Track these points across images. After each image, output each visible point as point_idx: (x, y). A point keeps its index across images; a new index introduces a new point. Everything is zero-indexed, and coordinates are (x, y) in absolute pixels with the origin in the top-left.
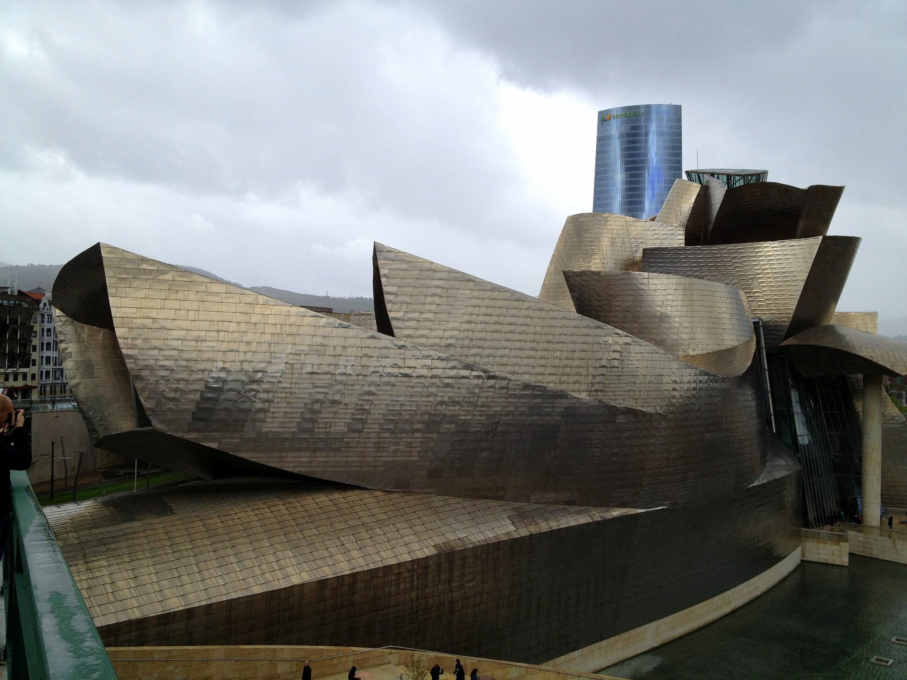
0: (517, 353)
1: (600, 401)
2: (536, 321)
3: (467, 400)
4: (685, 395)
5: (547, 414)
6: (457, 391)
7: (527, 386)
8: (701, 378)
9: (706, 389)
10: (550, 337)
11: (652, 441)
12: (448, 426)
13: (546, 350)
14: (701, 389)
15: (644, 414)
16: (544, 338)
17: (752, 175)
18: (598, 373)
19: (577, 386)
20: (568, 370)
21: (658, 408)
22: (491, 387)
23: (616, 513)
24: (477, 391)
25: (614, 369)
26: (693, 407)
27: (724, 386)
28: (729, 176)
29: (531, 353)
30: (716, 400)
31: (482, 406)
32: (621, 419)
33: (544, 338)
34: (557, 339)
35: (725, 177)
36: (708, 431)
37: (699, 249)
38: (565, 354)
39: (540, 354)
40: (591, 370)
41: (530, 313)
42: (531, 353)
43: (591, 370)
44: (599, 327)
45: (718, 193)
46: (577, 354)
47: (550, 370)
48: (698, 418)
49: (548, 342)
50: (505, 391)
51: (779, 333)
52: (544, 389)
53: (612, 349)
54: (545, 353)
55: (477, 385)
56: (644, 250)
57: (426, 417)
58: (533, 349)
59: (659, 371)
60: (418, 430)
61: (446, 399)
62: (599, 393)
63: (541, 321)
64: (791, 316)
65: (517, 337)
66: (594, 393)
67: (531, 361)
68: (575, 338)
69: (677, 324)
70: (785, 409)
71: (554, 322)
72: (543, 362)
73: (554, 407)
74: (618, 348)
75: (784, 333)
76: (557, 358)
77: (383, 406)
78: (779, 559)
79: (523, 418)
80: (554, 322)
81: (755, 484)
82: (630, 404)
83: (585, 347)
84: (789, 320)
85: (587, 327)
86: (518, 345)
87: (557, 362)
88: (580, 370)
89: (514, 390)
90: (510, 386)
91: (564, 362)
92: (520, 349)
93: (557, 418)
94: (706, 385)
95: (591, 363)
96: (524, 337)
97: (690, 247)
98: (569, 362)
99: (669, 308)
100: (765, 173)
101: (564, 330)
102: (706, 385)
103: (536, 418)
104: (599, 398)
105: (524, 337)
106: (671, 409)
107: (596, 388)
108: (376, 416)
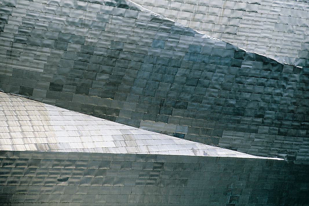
3: (96, 24)
5: (171, 48)
6: (87, 14)
7: (154, 19)
11: (278, 91)
12: (75, 46)
15: (274, 64)
18: (234, 15)
22: (121, 15)
24: (106, 17)
25: (253, 14)
31: (109, 32)
32: (247, 65)
40: (228, 12)
50: (132, 21)
55: (107, 12)
57: (56, 35)
60: (47, 46)
61: (77, 21)
62: (231, 36)
77: (20, 19)
79: (146, 49)
82: (260, 52)
89: (142, 21)
90: (138, 17)
93: (180, 54)
103: (158, 51)
107: (228, 30)
108: (11, 27)
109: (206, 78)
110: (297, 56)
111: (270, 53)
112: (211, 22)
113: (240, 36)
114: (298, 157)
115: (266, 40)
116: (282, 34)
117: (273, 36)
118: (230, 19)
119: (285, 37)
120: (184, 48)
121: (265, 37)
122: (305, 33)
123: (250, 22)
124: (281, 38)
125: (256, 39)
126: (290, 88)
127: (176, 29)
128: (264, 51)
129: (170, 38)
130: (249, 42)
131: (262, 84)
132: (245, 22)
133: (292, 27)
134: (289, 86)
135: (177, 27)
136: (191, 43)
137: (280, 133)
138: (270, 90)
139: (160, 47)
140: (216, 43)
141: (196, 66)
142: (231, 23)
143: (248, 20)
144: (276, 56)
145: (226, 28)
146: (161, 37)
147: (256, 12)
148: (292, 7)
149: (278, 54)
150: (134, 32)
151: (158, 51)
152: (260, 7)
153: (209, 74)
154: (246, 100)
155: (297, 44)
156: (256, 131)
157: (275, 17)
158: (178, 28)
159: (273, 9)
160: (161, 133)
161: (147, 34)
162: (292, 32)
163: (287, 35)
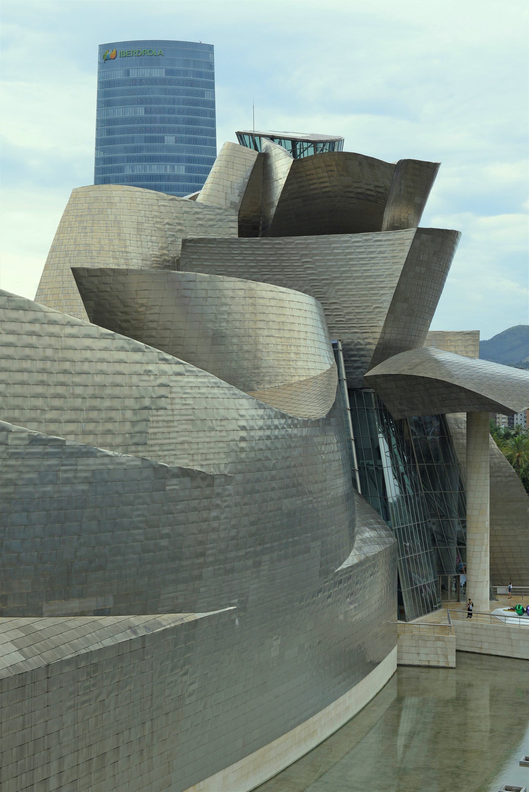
0: (18, 389)
1: (143, 459)
2: (47, 340)
4: (257, 447)
5: (67, 481)
7: (34, 441)
8: (276, 422)
9: (283, 437)
10: (67, 366)
11: (214, 514)
13: (63, 384)
14: (276, 437)
16: (57, 367)
17: (324, 142)
18: (138, 418)
19: (109, 439)
20: (94, 415)
21: (222, 467)
23: (168, 620)
25: (161, 412)
26: (267, 463)
27: (305, 431)
28: (294, 141)
29: (39, 389)
30: (295, 453)
33: (57, 367)
34: (78, 367)
35: (289, 143)
36: (287, 497)
37: (258, 243)
38: (90, 391)
39: (52, 390)
41: (36, 327)
42: (39, 389)
43: (129, 414)
44: (137, 350)
45: (282, 165)
46: (108, 391)
47: (69, 415)
48: (273, 478)
49: (65, 372)
51: (363, 359)
52: (62, 444)
53: (159, 381)
54: (60, 390)
56: (185, 241)
58: (42, 383)
59: (222, 412)
62: (140, 448)
63: (53, 341)
64: (378, 336)
65: (16, 365)
66: (133, 448)
67: (39, 402)
68: (104, 367)
69: (235, 348)
70: (372, 462)
71: (71, 342)
72: (57, 403)
73: (76, 471)
74: (163, 380)
75: (369, 359)
76: (76, 396)
78: (374, 664)
79: (31, 489)
80: (71, 342)
81: (344, 566)
82: (184, 462)
83: (119, 379)
84: (376, 342)
85: (122, 349)
86: (19, 377)
87: (78, 402)
88: (113, 414)
89: (16, 446)
90: (9, 442)
91: (89, 403)
92: (23, 383)
93: (81, 487)
94: (283, 432)
95: (130, 403)
96: (27, 365)
97: (246, 239)
98: (97, 403)
99: (224, 324)
100: (340, 141)
101: (88, 354)
102: (283, 432)
103: (49, 488)
104: (141, 454)
105: (27, 365)
106: (239, 467)
107: (135, 440)
110: (226, 461)
111: (195, 463)
112: (109, 432)
113: (151, 445)
115: (186, 446)
116: (201, 434)
117: (193, 438)
118: (133, 423)
119: (206, 437)
120: (86, 478)
121: (182, 443)
122: (227, 428)
123: (161, 424)
124: (202, 440)
125: (172, 447)
126: (226, 507)
127: (70, 450)
128: (186, 461)
129: (62, 465)
130: (166, 453)
131: (195, 509)
132: (155, 425)
133: (212, 422)
134: (225, 504)
135: (70, 446)
136: (94, 468)
137: (228, 572)
138: (205, 514)
139: (52, 482)
140: (127, 461)
142: (137, 428)
143: (158, 422)
144: (202, 465)
145: (132, 437)
146: (50, 466)
147: (166, 409)
148: (205, 396)
149: (204, 463)
150: (6, 466)
151: (49, 488)
152: (169, 401)
155: (221, 445)
156: (200, 577)
157: (190, 412)
158: (73, 448)
159: (184, 402)
160: (76, 615)
161: (29, 466)
162: (212, 429)
163: (208, 434)
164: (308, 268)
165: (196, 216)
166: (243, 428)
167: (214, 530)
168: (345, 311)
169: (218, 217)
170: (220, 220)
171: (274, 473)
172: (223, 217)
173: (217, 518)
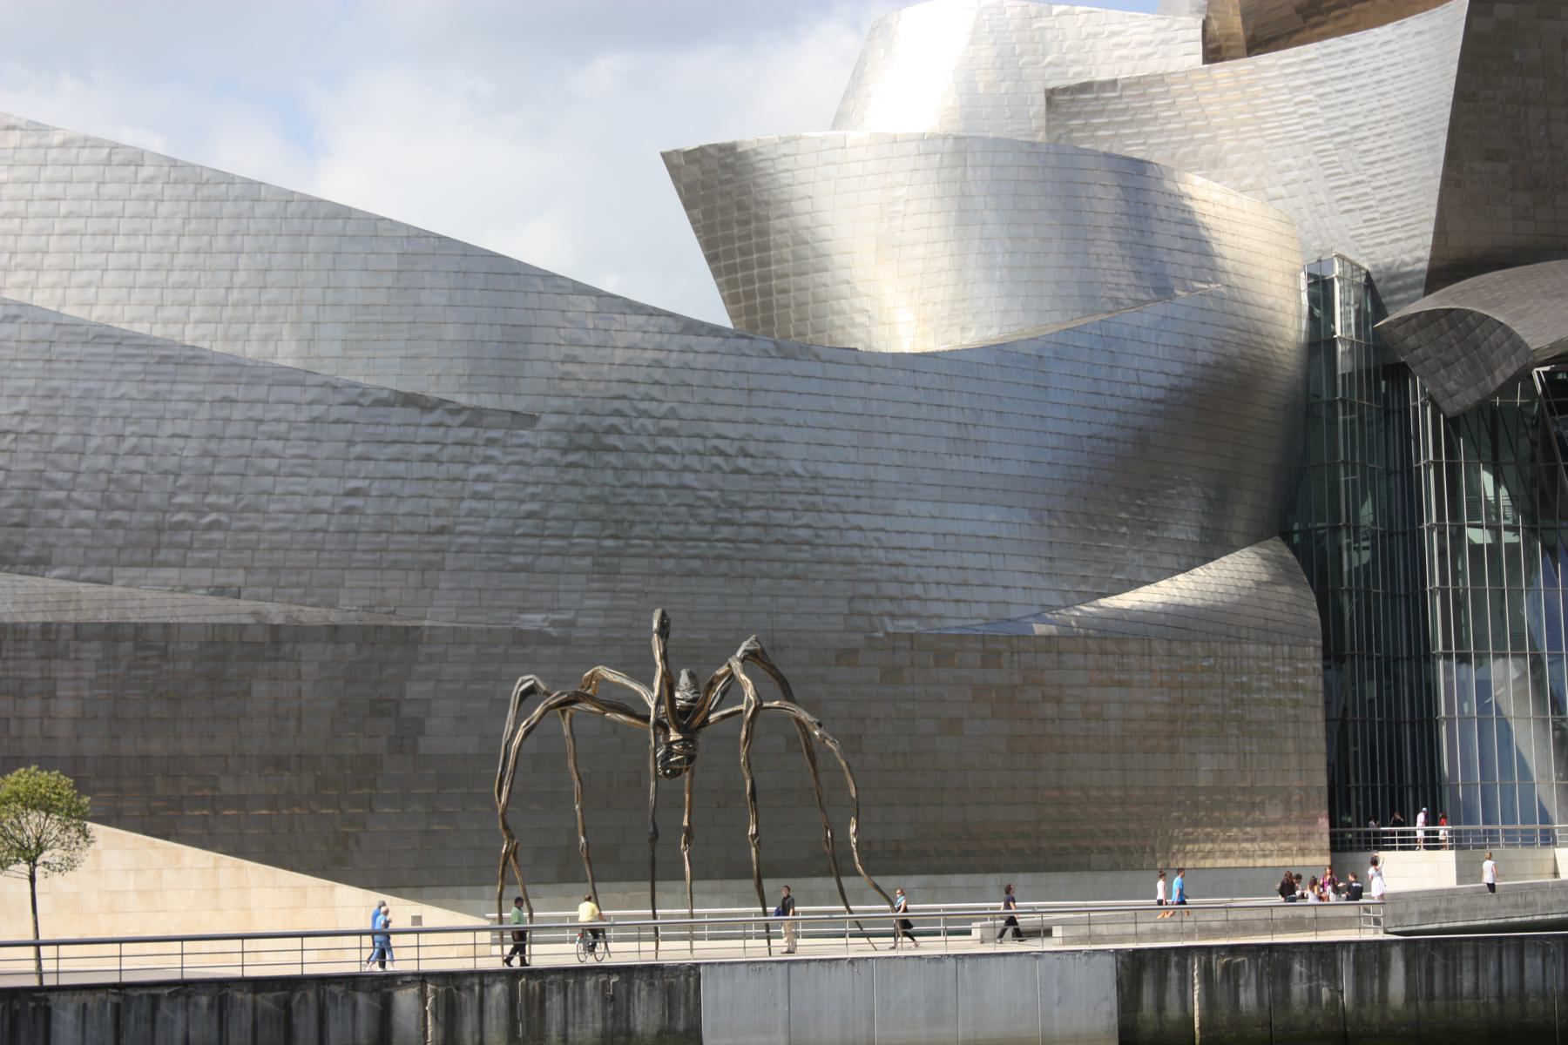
48: (670, 433)
56: (1051, 94)
109: (265, 454)
114: (582, 621)
120: (192, 393)
131: (428, 458)
138: (457, 469)
141: (233, 429)
153: (276, 446)
154: (391, 495)
161: (87, 371)
164: (1307, 115)
165: (1115, 40)
166: (573, 343)
167: (476, 496)
168: (1378, 197)
169: (1161, 36)
170: (1163, 42)
171: (673, 424)
172: (1170, 35)
173: (486, 478)
